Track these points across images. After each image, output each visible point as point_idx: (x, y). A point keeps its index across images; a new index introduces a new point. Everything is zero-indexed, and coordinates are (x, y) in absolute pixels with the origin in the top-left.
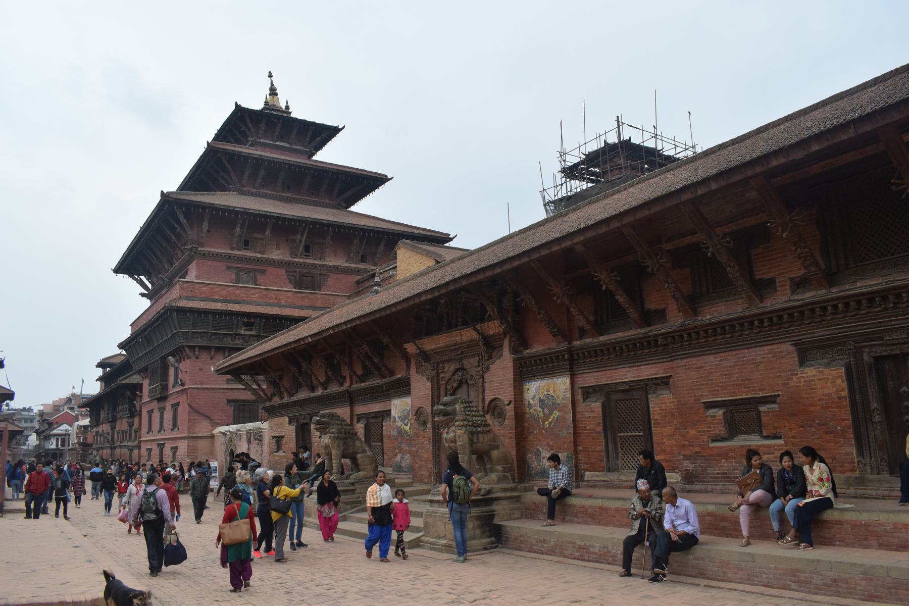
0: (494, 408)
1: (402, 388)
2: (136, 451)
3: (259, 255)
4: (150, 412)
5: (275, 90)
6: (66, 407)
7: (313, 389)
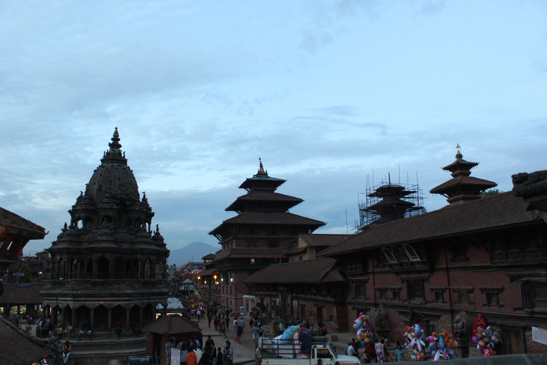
0: (288, 304)
1: (277, 296)
2: (219, 299)
3: (256, 236)
4: (223, 287)
5: (262, 165)
6: (187, 270)
7: (264, 291)
